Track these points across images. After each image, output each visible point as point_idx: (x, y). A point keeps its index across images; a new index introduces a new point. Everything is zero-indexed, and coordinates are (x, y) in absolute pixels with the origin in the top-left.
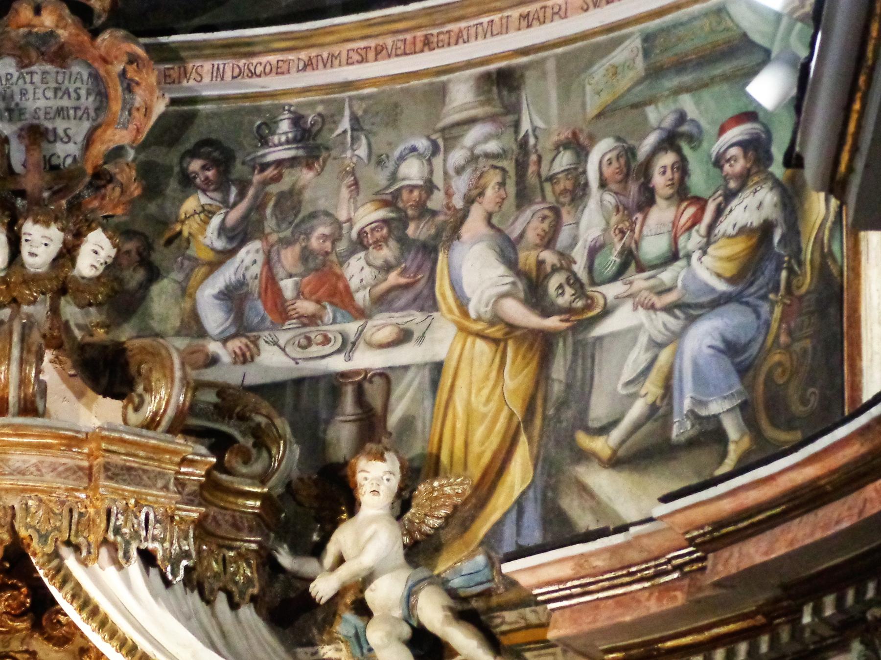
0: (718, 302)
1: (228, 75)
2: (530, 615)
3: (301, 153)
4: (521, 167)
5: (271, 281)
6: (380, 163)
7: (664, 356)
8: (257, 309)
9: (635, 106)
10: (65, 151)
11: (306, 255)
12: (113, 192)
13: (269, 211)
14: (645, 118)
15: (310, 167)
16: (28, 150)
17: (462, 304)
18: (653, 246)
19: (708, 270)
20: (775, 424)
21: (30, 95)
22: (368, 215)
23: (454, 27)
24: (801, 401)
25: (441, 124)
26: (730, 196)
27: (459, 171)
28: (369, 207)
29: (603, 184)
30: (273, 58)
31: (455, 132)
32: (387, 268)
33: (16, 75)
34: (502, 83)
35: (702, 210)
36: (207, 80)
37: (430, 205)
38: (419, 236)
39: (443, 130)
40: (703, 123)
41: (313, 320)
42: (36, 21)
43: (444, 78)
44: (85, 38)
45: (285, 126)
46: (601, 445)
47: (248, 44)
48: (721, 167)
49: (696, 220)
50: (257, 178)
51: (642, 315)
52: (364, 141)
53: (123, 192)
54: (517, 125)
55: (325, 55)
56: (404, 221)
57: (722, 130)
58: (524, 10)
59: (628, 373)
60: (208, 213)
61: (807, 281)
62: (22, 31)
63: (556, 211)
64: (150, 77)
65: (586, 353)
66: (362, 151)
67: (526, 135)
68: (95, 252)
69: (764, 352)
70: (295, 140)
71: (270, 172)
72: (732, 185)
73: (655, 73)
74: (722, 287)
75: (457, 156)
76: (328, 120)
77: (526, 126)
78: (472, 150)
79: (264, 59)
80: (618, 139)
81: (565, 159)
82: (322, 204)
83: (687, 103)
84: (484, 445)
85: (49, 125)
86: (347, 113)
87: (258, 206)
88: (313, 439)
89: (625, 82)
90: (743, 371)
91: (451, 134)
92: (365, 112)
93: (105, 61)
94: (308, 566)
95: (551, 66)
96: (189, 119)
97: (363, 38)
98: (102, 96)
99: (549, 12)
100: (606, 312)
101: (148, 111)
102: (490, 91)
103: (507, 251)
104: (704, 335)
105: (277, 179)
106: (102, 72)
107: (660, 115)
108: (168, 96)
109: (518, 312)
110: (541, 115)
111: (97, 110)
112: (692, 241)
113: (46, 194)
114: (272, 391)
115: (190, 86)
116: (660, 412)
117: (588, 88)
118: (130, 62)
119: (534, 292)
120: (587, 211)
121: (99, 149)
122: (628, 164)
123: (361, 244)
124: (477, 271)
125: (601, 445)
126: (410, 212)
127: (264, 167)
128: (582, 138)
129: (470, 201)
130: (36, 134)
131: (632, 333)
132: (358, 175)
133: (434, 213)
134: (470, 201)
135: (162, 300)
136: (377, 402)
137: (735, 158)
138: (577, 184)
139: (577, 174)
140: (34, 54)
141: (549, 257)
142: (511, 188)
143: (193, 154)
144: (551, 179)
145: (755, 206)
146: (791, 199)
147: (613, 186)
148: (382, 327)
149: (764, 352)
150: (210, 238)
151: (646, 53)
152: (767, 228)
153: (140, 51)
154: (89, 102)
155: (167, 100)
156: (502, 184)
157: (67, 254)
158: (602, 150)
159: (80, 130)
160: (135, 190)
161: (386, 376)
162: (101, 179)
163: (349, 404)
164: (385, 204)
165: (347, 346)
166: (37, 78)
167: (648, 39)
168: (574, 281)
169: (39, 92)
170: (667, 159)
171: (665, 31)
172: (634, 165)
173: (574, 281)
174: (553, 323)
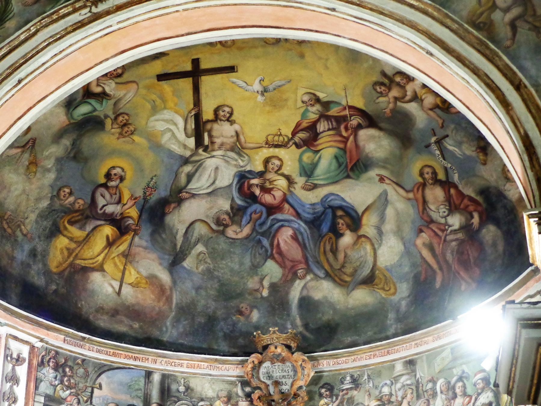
1: (331, 364)
3: (353, 386)
4: (417, 387)
6: (376, 388)
9: (450, 369)
10: (285, 388)
12: (299, 399)
13: (345, 403)
14: (453, 372)
15: (356, 390)
16: (274, 388)
21: (275, 372)
23: (396, 348)
25: (393, 376)
26: (479, 394)
27: (399, 390)
28: (374, 401)
29: (441, 392)
30: (344, 359)
31: (397, 378)
33: (271, 366)
34: (411, 363)
35: (471, 399)
36: (325, 366)
37: (392, 400)
39: (394, 378)
40: (470, 373)
42: (276, 350)
43: (394, 363)
44: (290, 355)
45: (348, 378)
47: (337, 355)
48: (476, 386)
49: (469, 402)
50: (341, 394)
52: (371, 382)
53: (302, 399)
54: (415, 376)
55: (359, 357)
57: (475, 375)
58: (416, 342)
62: (272, 354)
63: (428, 400)
64: (309, 365)
66: (371, 385)
67: (418, 379)
70: (351, 382)
71: (345, 392)
72: (479, 391)
75: (399, 385)
77: (418, 376)
78: (403, 383)
79: (341, 359)
80: (445, 379)
81: (430, 385)
82: (360, 401)
85: (280, 380)
86: (366, 373)
89: (446, 362)
91: (397, 379)
92: (372, 373)
93: (296, 361)
95: (424, 358)
96: (320, 378)
97: (369, 352)
98: (295, 371)
99: (423, 342)
101: (309, 375)
102: (407, 366)
105: (347, 394)
106: (295, 365)
108: (314, 371)
110: (423, 372)
111: (294, 375)
113: (280, 401)
115: (320, 368)
117: (436, 364)
118: (303, 361)
120: (437, 400)
121: (296, 387)
122: (448, 386)
126: (386, 402)
127: (343, 390)
128: (435, 379)
129: (403, 398)
130: (277, 383)
132: (370, 391)
133: (393, 402)
134: (403, 398)
137: (479, 383)
138: (434, 392)
139: (434, 389)
140: (275, 360)
142: (415, 394)
143: (322, 387)
144: (426, 391)
146: (497, 396)
147: (445, 393)
151: (452, 353)
153: (306, 358)
154: (291, 373)
155: (314, 372)
156: (412, 393)
158: (440, 383)
160: (306, 398)
162: (296, 396)
164: (379, 400)
166: (276, 367)
167: (452, 349)
169: (277, 372)
170: (460, 384)
172: (450, 386)
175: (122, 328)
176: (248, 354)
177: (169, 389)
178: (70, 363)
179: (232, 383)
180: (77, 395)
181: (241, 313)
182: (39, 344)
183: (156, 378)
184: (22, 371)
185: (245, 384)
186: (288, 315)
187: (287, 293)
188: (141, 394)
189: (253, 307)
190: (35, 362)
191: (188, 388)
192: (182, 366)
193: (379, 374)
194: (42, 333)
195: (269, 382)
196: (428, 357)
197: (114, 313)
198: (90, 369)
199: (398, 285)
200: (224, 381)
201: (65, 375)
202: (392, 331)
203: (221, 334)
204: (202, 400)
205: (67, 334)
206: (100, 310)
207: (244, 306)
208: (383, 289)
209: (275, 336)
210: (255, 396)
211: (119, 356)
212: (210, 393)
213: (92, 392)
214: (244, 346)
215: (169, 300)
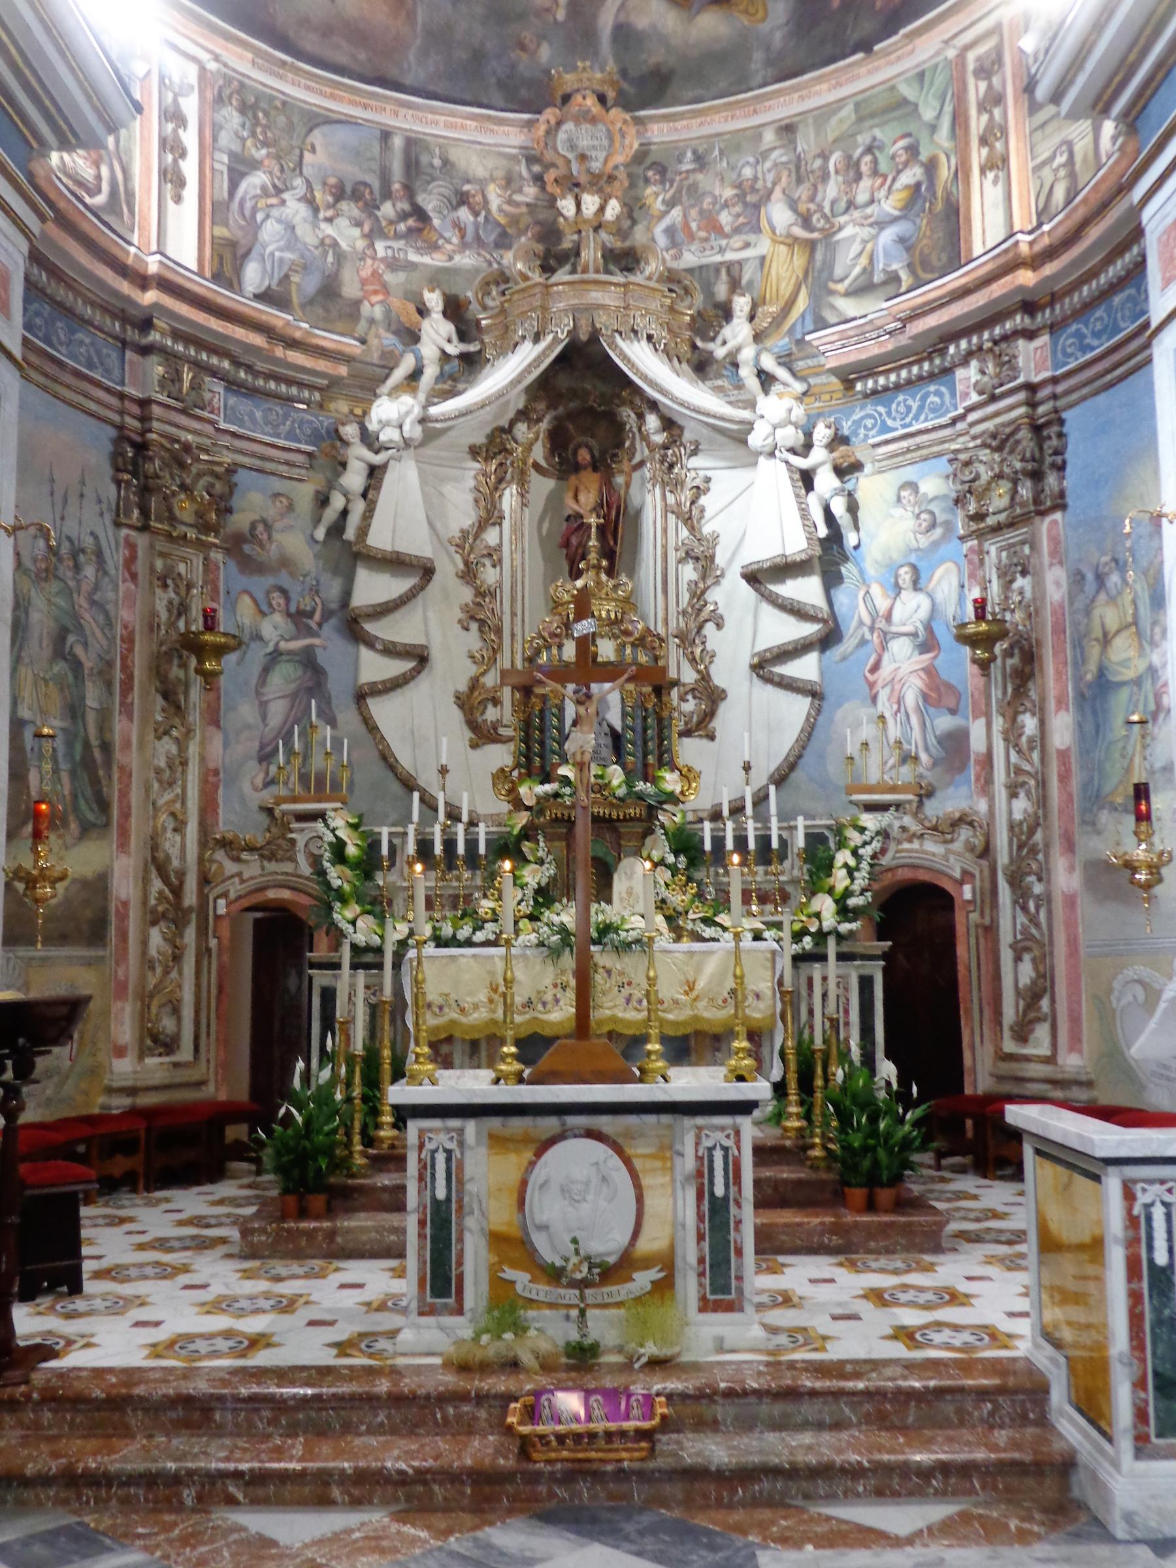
0: (894, 220)
2: (810, 362)
4: (798, 167)
5: (686, 224)
7: (869, 246)
8: (680, 236)
10: (596, 166)
11: (701, 212)
12: (617, 184)
17: (773, 230)
18: (862, 197)
19: (889, 206)
20: (925, 271)
22: (729, 193)
24: (939, 259)
26: (899, 172)
32: (738, 216)
34: (788, 129)
38: (752, 200)
41: (706, 240)
45: (689, 154)
46: (841, 287)
51: (857, 229)
56: (744, 195)
59: (852, 254)
60: (657, 195)
61: (939, 206)
63: (815, 187)
64: (632, 130)
65: (832, 248)
68: (613, 209)
69: (919, 240)
73: (860, 119)
74: (896, 213)
76: (709, 151)
81: (818, 163)
83: (877, 132)
84: (786, 290)
87: (679, 191)
88: (709, 293)
89: (845, 127)
90: (908, 249)
91: (765, 155)
94: (710, 346)
98: (611, 139)
100: (840, 229)
103: (793, 205)
104: (888, 235)
107: (863, 139)
109: (798, 232)
110: (806, 143)
112: (882, 193)
114: (690, 271)
116: (868, 271)
119: (806, 221)
121: (610, 164)
123: (726, 205)
124: (779, 215)
125: (841, 287)
129: (774, 184)
130: (583, 157)
131: (852, 238)
134: (774, 184)
135: (639, 236)
136: (735, 273)
141: (812, 207)
145: (912, 175)
148: (737, 241)
149: (919, 240)
150: (658, 205)
152: (918, 185)
154: (605, 142)
157: (602, 209)
158: (835, 158)
159: (602, 155)
161: (740, 263)
162: (611, 178)
163: (723, 275)
165: (722, 251)
167: (857, 105)
168: (825, 216)
170: (868, 158)
171: (864, 101)
173: (825, 216)
174: (815, 235)
175: (342, 59)
176: (539, 112)
177: (417, 162)
178: (263, 105)
179: (512, 158)
180: (278, 158)
181: (523, 47)
182: (212, 66)
183: (397, 142)
184: (190, 106)
185: (531, 160)
186: (596, 54)
187: (595, 17)
188: (375, 166)
189: (542, 37)
190: (209, 96)
191: (446, 162)
192: (437, 123)
193: (738, 148)
194: (218, 45)
195: (570, 156)
196: (816, 119)
197: (327, 31)
198: (295, 119)
199: (770, 5)
200: (500, 154)
201: (257, 122)
202: (759, 79)
203: (493, 80)
204: (468, 181)
205: (257, 52)
206: (305, 22)
207: (527, 36)
208: (746, 12)
209: (585, 75)
210: (550, 176)
211: (340, 100)
212: (480, 172)
213: (301, 156)
214: (531, 95)
215: (411, 16)
